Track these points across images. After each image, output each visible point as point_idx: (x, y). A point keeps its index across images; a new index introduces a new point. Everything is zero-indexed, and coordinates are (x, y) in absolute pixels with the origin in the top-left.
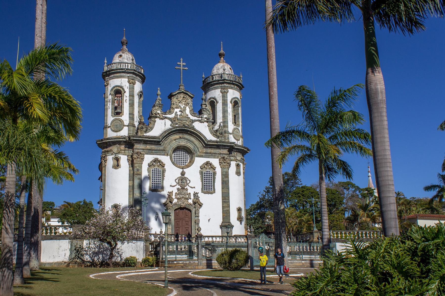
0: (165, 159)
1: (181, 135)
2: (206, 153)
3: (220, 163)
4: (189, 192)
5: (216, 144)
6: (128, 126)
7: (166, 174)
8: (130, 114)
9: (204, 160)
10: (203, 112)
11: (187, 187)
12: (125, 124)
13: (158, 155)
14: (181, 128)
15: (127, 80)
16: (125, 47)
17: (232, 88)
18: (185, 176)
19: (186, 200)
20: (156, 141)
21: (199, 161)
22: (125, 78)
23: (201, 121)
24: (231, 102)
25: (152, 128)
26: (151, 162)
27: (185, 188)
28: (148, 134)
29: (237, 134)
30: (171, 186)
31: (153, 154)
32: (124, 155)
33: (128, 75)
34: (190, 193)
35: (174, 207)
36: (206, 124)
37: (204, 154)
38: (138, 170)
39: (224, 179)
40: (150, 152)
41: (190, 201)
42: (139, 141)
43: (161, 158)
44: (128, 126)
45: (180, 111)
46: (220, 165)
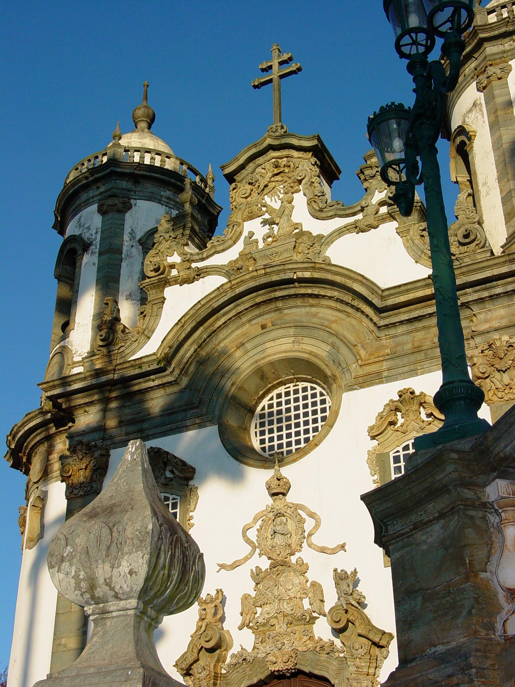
2: (394, 356)
9: (387, 392)
11: (306, 554)
18: (291, 498)
27: (293, 559)
35: (234, 676)
37: (385, 365)
41: (322, 630)
45: (265, 223)
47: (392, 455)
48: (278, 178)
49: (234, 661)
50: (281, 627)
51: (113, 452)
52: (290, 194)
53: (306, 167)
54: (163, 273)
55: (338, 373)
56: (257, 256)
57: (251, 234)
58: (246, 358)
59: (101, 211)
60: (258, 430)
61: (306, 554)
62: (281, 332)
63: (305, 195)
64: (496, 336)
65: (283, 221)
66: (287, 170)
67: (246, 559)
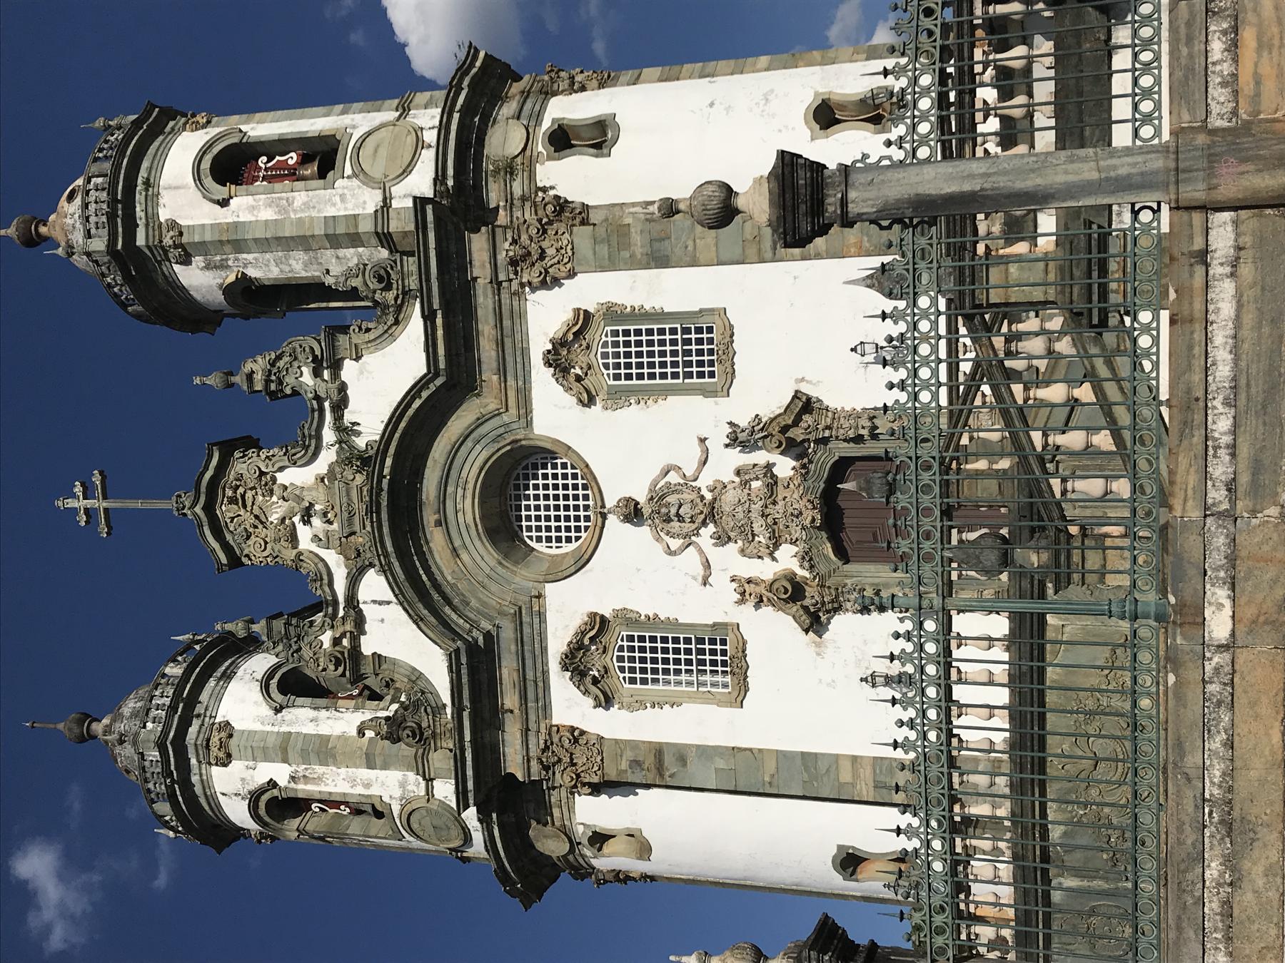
0: (565, 611)
1: (429, 517)
2: (502, 371)
3: (544, 285)
4: (728, 476)
5: (439, 321)
6: (429, 780)
7: (645, 608)
8: (371, 766)
9: (542, 380)
10: (288, 391)
11: (704, 482)
12: (423, 793)
13: (544, 650)
14: (386, 530)
15: (216, 771)
16: (98, 728)
17: (153, 199)
18: (642, 498)
19: (781, 492)
20: (477, 665)
21: (553, 412)
22: (210, 776)
23: (340, 405)
24: (224, 203)
25: (416, 677)
26: (586, 692)
27: (709, 496)
28: (446, 698)
29: (383, 152)
30: (705, 583)
31: (545, 673)
32: (571, 810)
33: (193, 761)
34: (738, 473)
35: (822, 568)
36: (349, 370)
37: (511, 382)
38: (636, 764)
39: (639, 251)
40: (535, 693)
41: (785, 467)
42: (487, 751)
43: (558, 642)
44: (429, 780)
45: (306, 520)
46: (556, 282)
47: (611, 382)
48: (249, 503)
49: (806, 564)
50: (777, 511)
51: (556, 721)
52: (275, 487)
53: (244, 466)
54: (342, 653)
55: (509, 438)
56: (347, 531)
57: (316, 539)
58: (471, 548)
59: (225, 761)
60: (554, 544)
61: (704, 482)
62: (449, 504)
63: (281, 469)
64: (499, 257)
65: (308, 498)
66: (241, 490)
67: (701, 552)
